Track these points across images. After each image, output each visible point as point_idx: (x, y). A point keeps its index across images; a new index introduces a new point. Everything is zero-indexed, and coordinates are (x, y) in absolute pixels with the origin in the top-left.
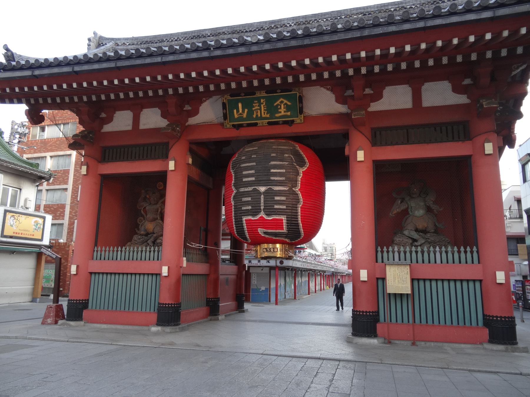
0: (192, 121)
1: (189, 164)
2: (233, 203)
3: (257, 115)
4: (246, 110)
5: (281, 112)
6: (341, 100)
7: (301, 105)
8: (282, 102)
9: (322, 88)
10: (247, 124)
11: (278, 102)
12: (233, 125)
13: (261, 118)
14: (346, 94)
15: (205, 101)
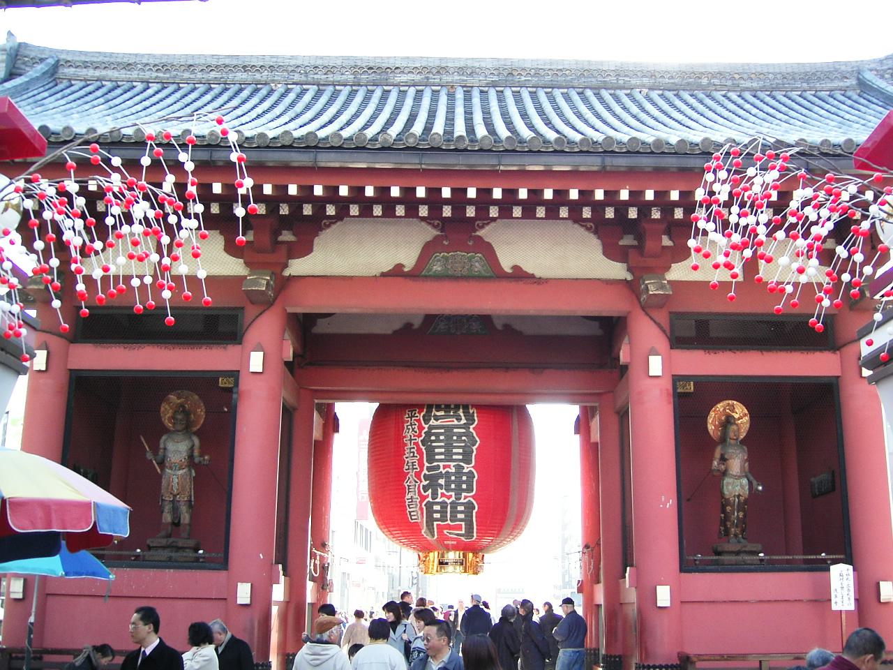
6: (612, 252)
9: (576, 226)
14: (621, 243)
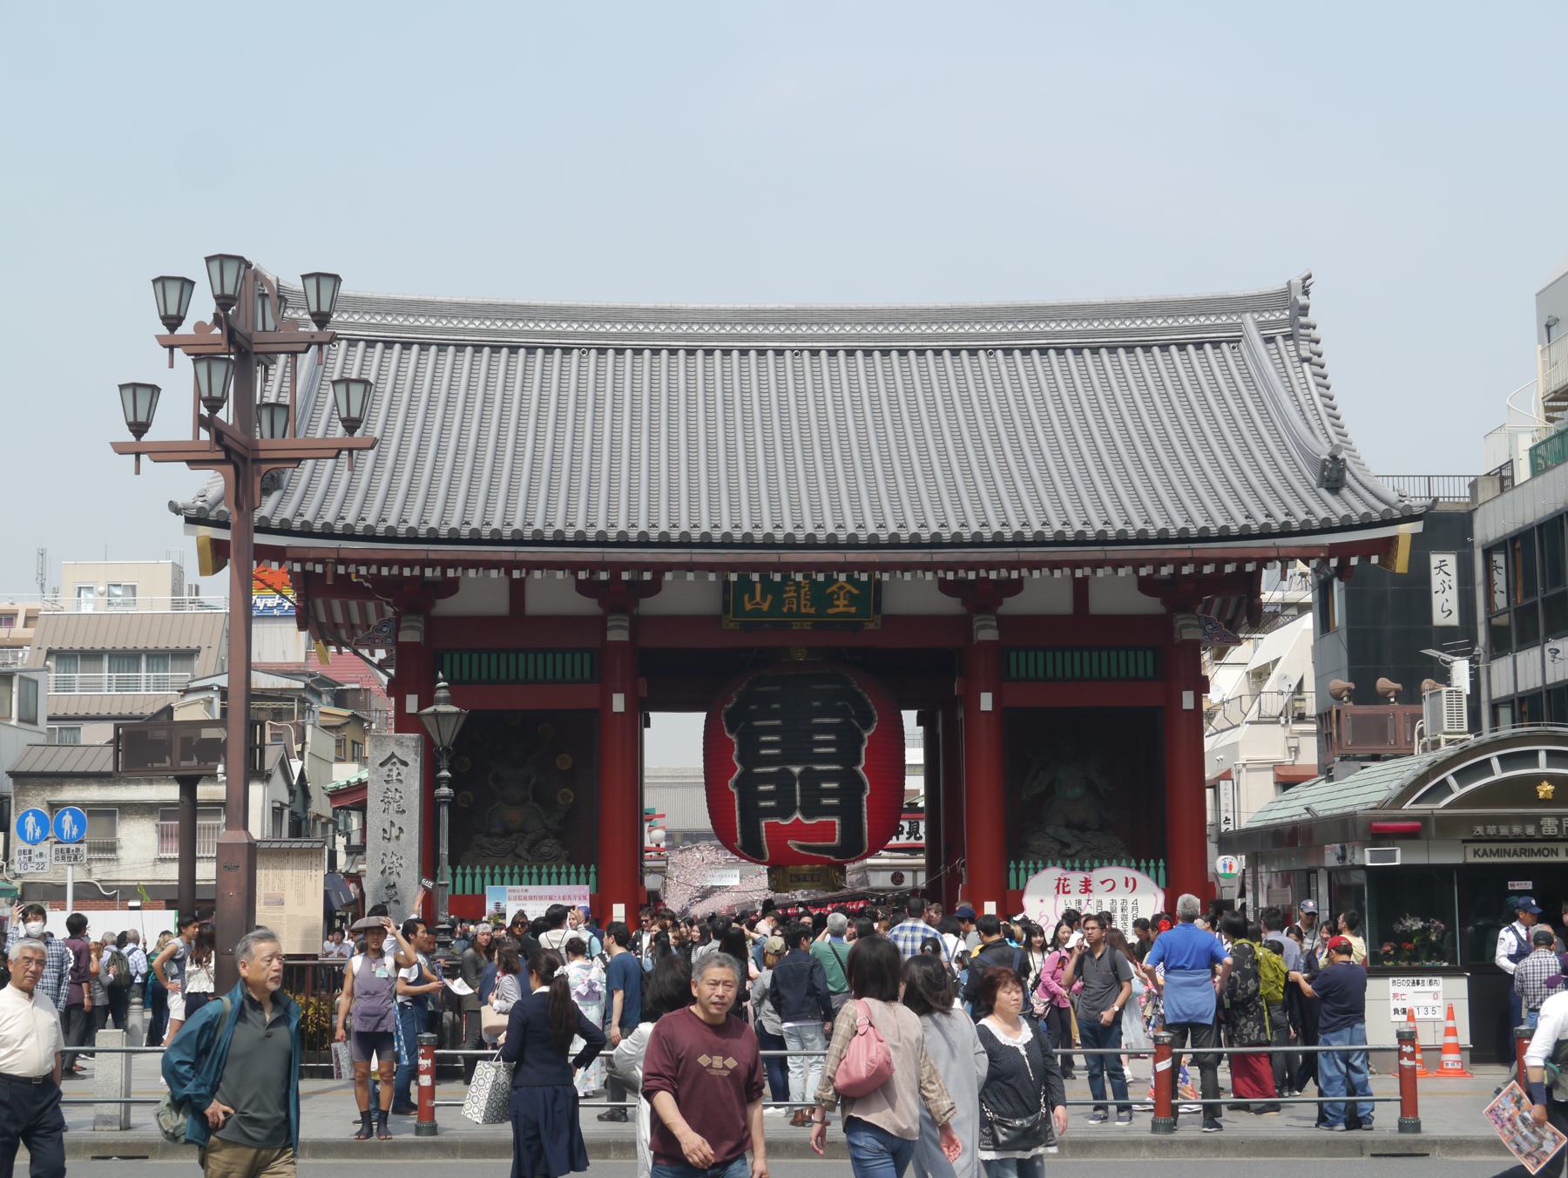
4: (770, 597)
8: (841, 588)
11: (834, 588)
13: (799, 614)
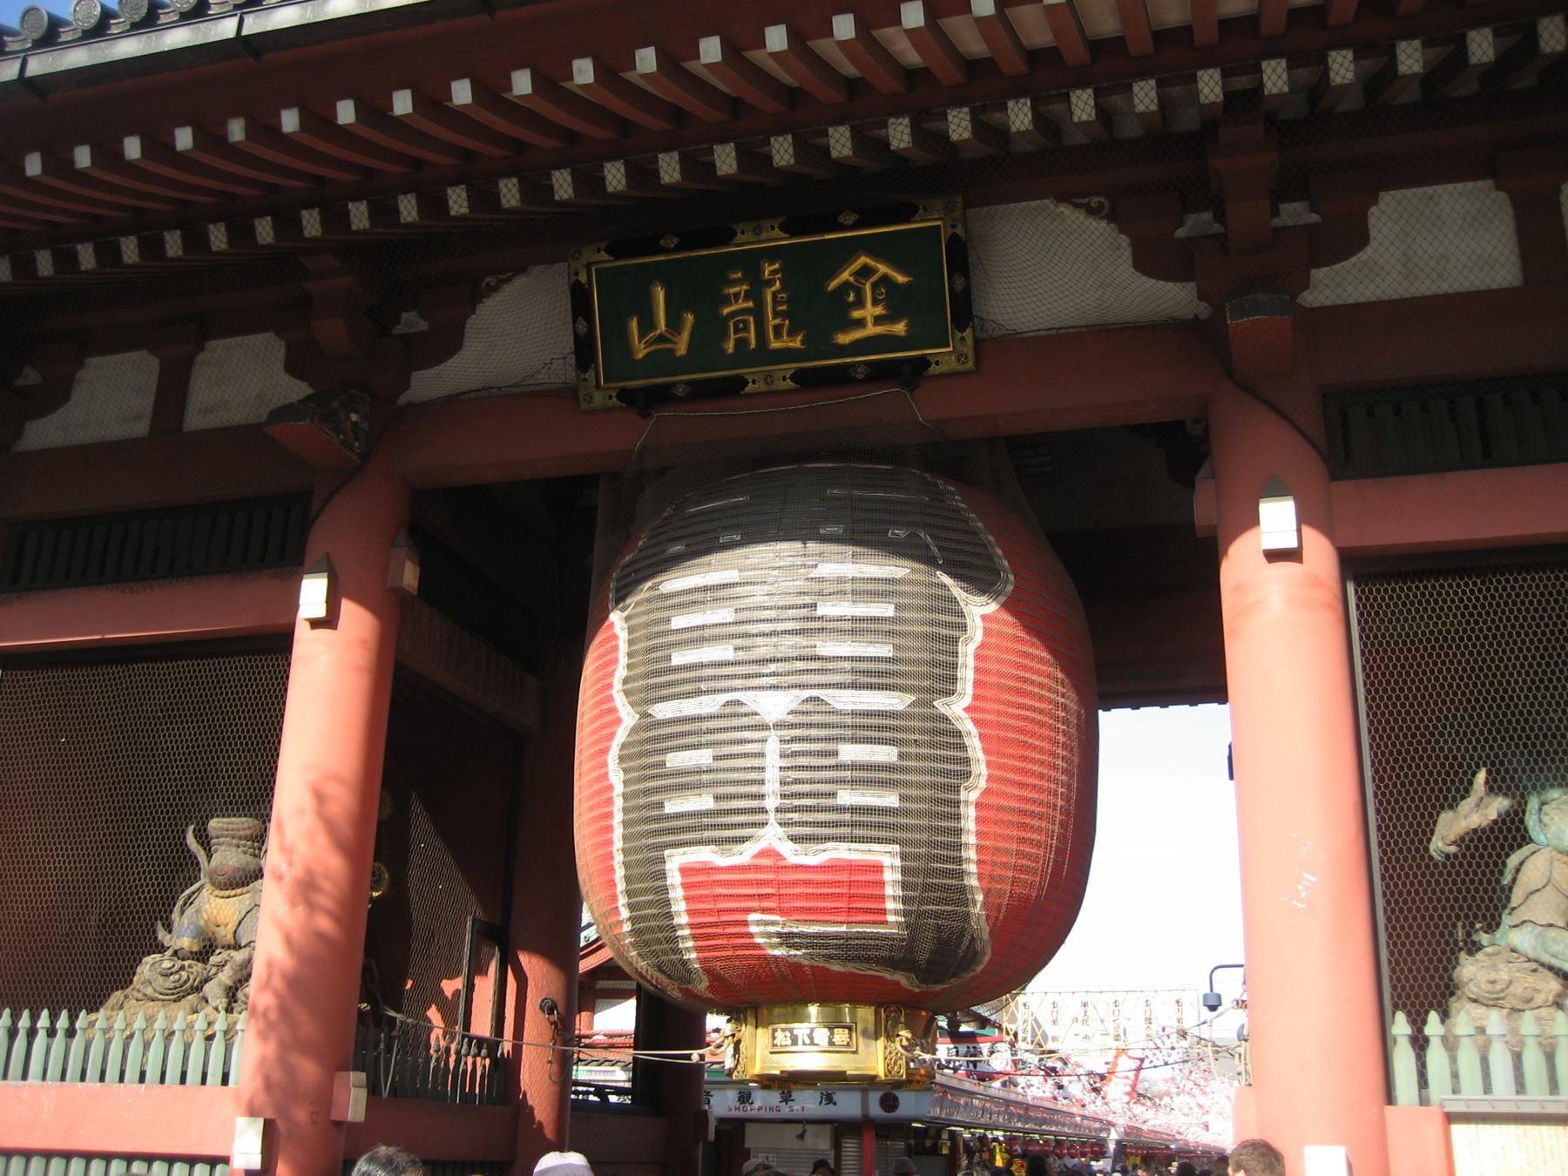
0: (427, 384)
1: (400, 594)
2: (616, 777)
3: (741, 343)
5: (861, 323)
6: (1152, 259)
7: (959, 283)
8: (866, 272)
9: (1065, 209)
10: (689, 383)
11: (845, 276)
12: (623, 395)
15: (493, 290)
